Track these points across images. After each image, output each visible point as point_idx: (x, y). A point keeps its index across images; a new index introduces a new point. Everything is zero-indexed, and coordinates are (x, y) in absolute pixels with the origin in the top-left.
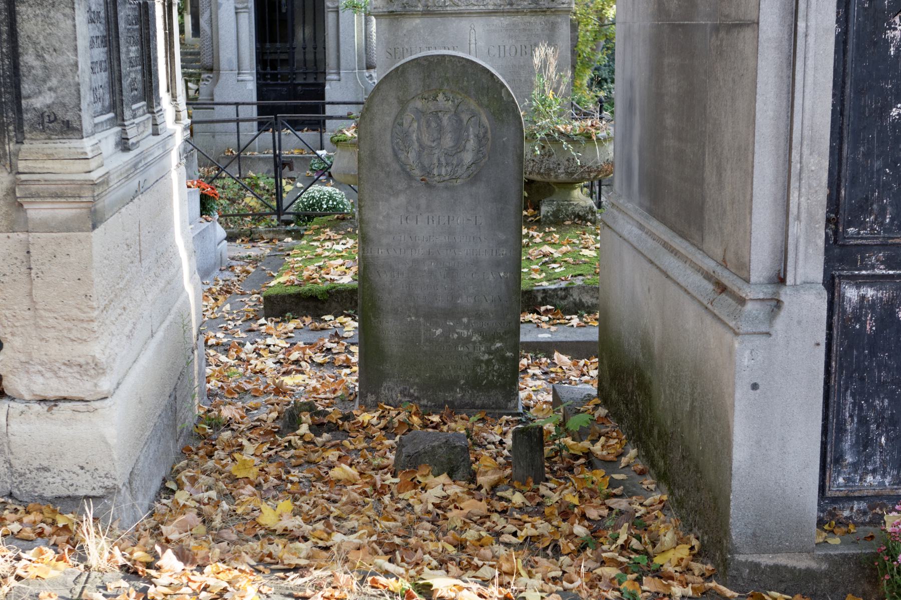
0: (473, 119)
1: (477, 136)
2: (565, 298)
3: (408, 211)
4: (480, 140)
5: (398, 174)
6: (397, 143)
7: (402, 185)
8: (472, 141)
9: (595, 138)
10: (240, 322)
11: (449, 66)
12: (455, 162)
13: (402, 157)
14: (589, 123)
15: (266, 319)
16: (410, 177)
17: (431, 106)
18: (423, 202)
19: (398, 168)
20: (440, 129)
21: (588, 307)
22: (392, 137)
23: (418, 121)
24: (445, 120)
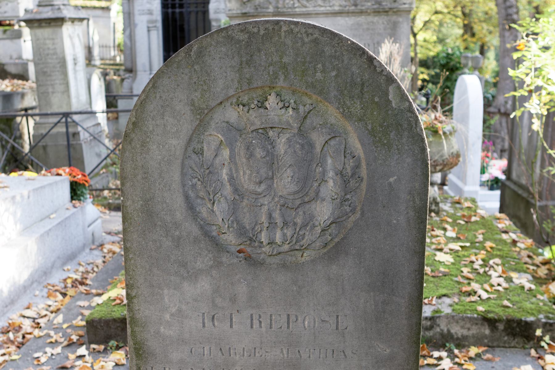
0: (332, 143)
1: (340, 173)
2: (431, 328)
3: (214, 305)
4: (347, 180)
5: (196, 240)
6: (194, 186)
7: (204, 261)
8: (331, 183)
9: (441, 132)
10: (59, 350)
11: (288, 42)
12: (299, 221)
13: (204, 212)
14: (433, 116)
15: (88, 349)
16: (217, 246)
17: (255, 118)
18: (242, 290)
19: (196, 231)
20: (272, 160)
21: (458, 339)
23: (231, 145)
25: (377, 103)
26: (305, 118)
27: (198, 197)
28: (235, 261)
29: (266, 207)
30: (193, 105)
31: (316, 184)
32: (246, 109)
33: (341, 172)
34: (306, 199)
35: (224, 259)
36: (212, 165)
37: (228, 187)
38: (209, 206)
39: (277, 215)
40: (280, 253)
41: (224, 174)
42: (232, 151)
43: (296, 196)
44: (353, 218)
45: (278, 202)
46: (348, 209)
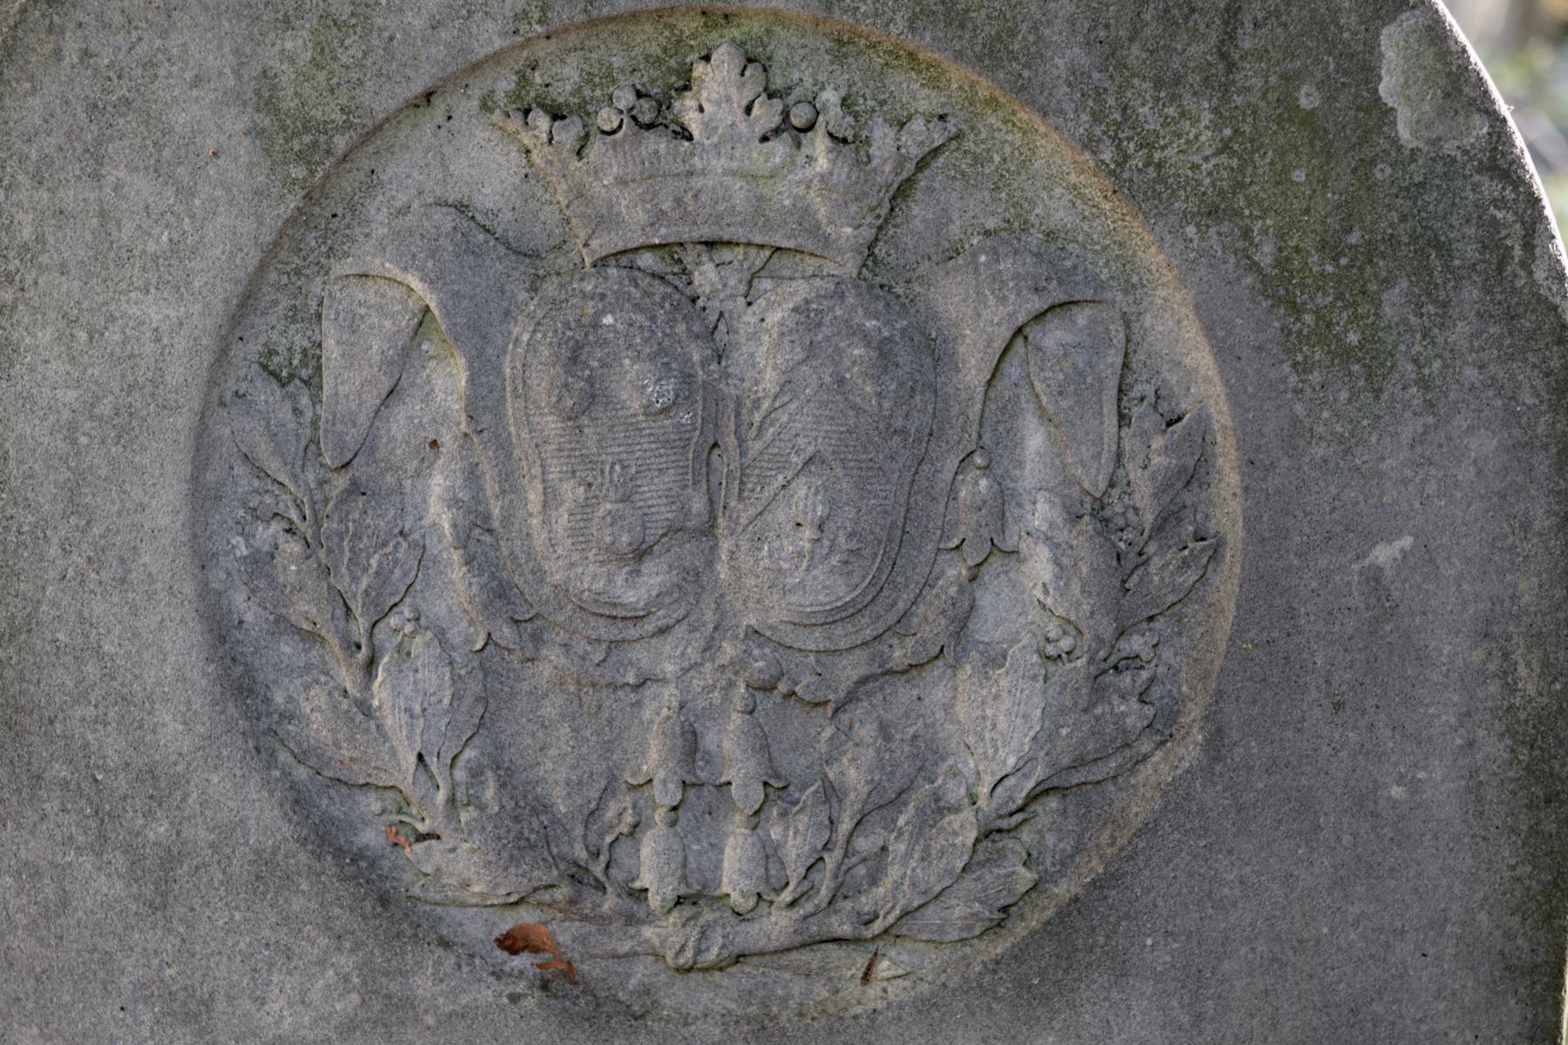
0: (1053, 336)
1: (1095, 512)
4: (1134, 549)
5: (266, 874)
6: (261, 563)
8: (1040, 566)
12: (854, 775)
13: (316, 714)
16: (387, 907)
17: (617, 190)
19: (264, 819)
20: (708, 431)
22: (202, 496)
24: (764, 341)
25: (1309, 119)
26: (903, 191)
27: (281, 625)
28: (487, 993)
29: (670, 695)
30: (268, 102)
31: (955, 571)
32: (568, 134)
33: (1100, 504)
34: (899, 655)
35: (423, 985)
36: (368, 446)
37: (457, 573)
38: (347, 677)
39: (728, 741)
40: (739, 958)
41: (436, 502)
42: (483, 371)
43: (843, 636)
44: (1159, 768)
45: (739, 665)
46: (1133, 714)
